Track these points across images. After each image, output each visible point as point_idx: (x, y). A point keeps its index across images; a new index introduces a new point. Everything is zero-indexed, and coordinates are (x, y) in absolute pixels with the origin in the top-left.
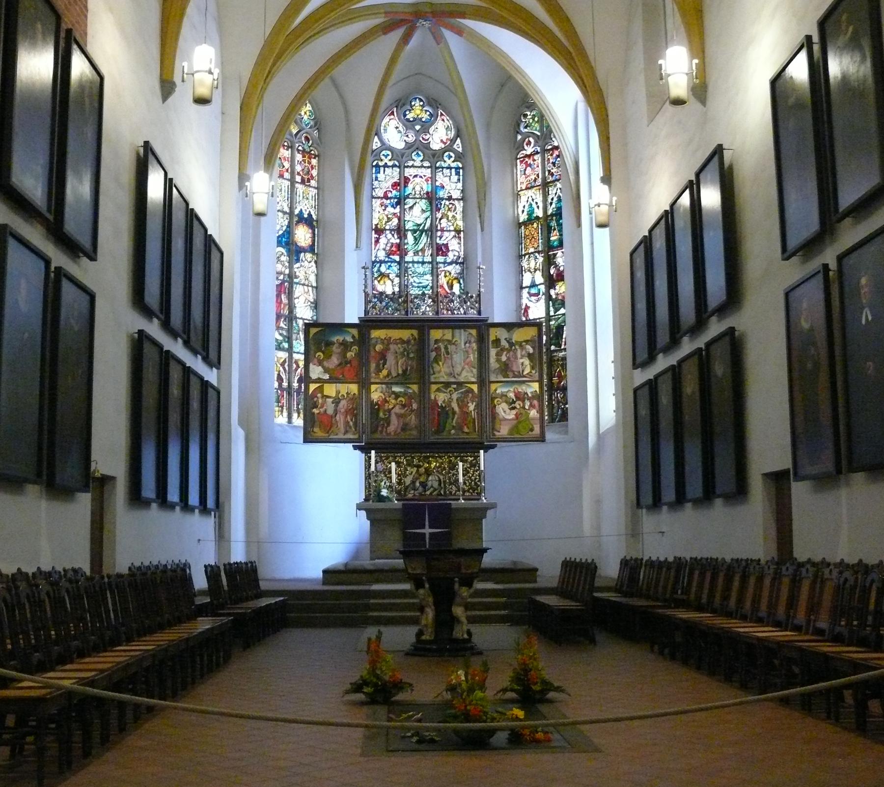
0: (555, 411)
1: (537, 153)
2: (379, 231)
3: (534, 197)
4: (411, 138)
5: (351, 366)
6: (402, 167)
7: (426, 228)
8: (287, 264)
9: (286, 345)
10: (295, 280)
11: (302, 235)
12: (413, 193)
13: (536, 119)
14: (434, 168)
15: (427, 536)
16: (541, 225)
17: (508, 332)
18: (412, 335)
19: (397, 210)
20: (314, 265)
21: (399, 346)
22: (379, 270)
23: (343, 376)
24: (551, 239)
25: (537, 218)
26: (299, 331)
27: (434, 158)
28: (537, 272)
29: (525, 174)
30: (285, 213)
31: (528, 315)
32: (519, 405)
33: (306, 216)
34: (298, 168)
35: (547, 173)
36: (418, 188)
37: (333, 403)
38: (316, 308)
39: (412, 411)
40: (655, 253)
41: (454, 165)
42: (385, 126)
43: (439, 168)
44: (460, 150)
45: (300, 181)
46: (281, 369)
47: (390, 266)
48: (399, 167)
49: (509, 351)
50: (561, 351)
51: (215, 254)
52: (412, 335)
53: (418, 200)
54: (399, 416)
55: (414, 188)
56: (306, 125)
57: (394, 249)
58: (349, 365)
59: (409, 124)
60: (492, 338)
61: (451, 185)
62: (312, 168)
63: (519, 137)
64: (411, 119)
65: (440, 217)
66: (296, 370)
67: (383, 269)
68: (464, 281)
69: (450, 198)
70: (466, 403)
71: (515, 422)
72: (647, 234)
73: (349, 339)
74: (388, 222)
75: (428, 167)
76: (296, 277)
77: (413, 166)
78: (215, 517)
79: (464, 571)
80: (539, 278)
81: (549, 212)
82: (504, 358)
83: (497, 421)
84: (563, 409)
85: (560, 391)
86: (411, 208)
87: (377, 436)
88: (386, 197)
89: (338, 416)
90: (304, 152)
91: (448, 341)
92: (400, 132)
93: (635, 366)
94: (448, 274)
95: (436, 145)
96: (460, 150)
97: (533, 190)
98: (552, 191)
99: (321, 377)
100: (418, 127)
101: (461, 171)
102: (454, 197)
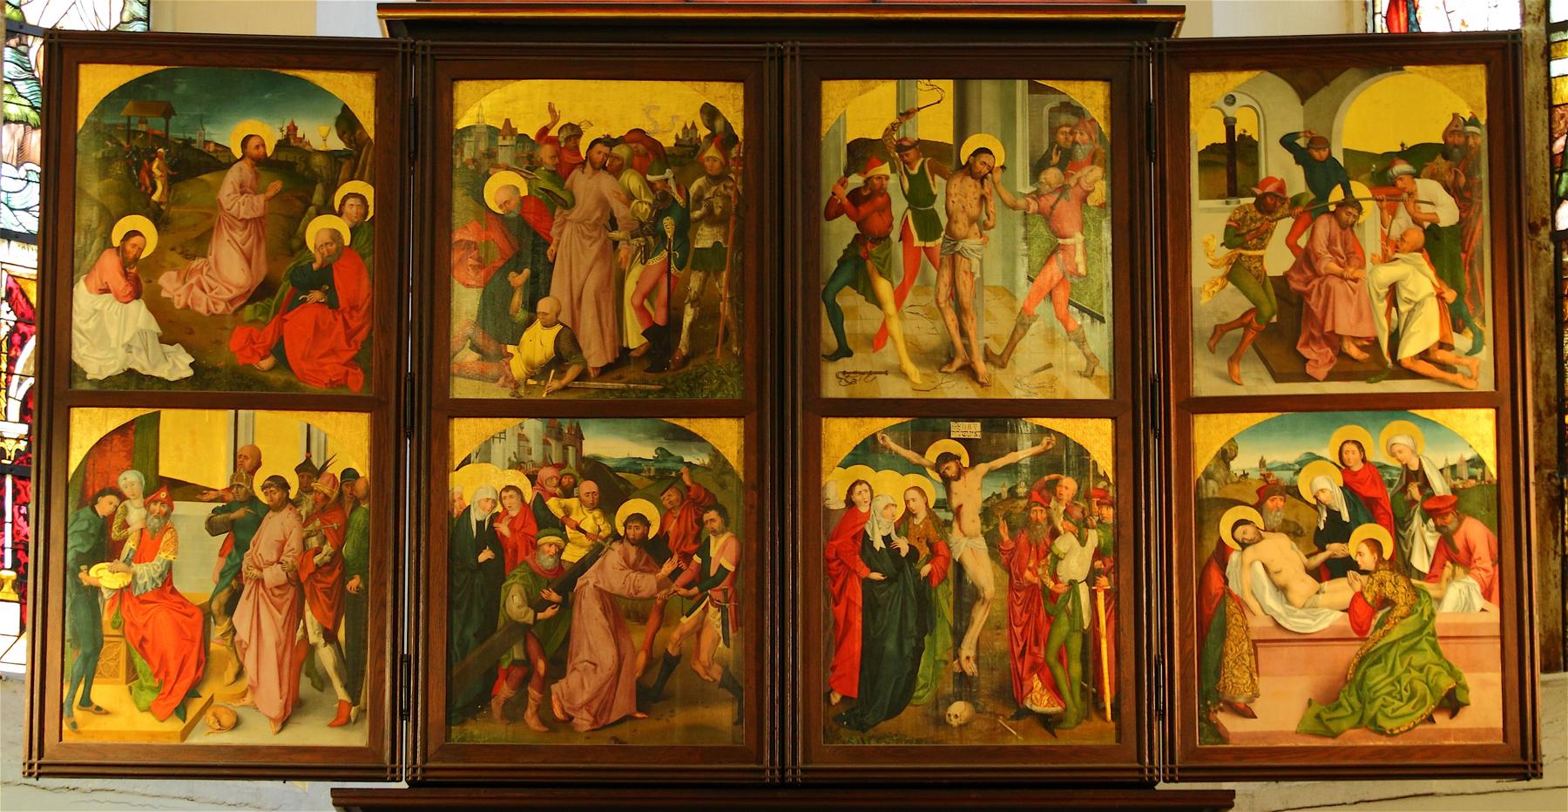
5: (332, 303)
17: (1304, 96)
18: (710, 113)
21: (632, 180)
23: (282, 362)
32: (1375, 545)
37: (213, 528)
39: (704, 580)
49: (1310, 211)
52: (710, 113)
54: (621, 612)
58: (316, 296)
60: (1206, 131)
70: (1042, 532)
71: (1350, 651)
73: (320, 135)
82: (1277, 259)
83: (1235, 648)
87: (486, 731)
89: (244, 609)
91: (924, 147)
99: (142, 364)
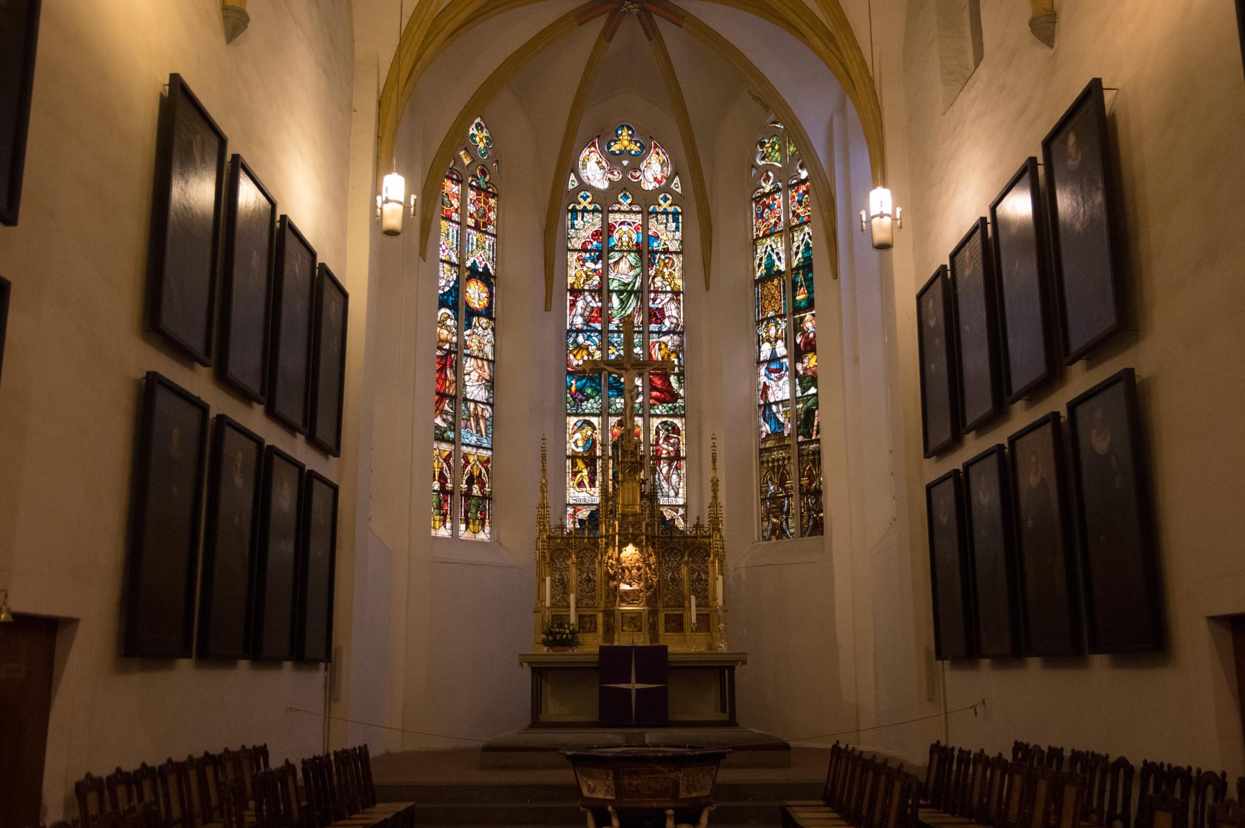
0: (804, 521)
1: (778, 190)
2: (576, 292)
3: (774, 247)
4: (617, 177)
6: (605, 212)
7: (635, 289)
8: (454, 330)
9: (451, 435)
10: (465, 351)
11: (476, 294)
12: (620, 244)
13: (777, 147)
14: (645, 213)
15: (634, 693)
16: (784, 280)
19: (599, 266)
20: (491, 332)
22: (575, 342)
24: (798, 298)
25: (779, 273)
26: (470, 417)
27: (645, 203)
28: (779, 342)
29: (762, 217)
30: (452, 264)
31: (767, 397)
33: (481, 270)
34: (472, 209)
35: (791, 215)
36: (625, 238)
38: (492, 387)
40: (959, 290)
41: (671, 209)
42: (584, 161)
43: (651, 213)
44: (679, 190)
45: (473, 225)
46: (445, 465)
47: (589, 336)
48: (601, 212)
50: (812, 442)
51: (329, 292)
53: (625, 254)
55: (620, 238)
56: (483, 155)
57: (594, 314)
59: (613, 160)
61: (667, 235)
62: (490, 211)
63: (754, 172)
64: (617, 152)
65: (653, 274)
66: (465, 466)
67: (581, 339)
68: (683, 355)
69: (666, 251)
72: (947, 262)
74: (587, 280)
75: (638, 212)
76: (467, 347)
77: (619, 211)
78: (326, 669)
79: (683, 794)
80: (781, 349)
81: (795, 264)
84: (815, 519)
85: (811, 494)
86: (617, 263)
88: (584, 249)
90: (478, 189)
92: (602, 168)
93: (928, 453)
94: (663, 346)
95: (649, 186)
96: (679, 190)
97: (773, 238)
98: (798, 237)
100: (625, 163)
101: (680, 217)
102: (672, 249)
